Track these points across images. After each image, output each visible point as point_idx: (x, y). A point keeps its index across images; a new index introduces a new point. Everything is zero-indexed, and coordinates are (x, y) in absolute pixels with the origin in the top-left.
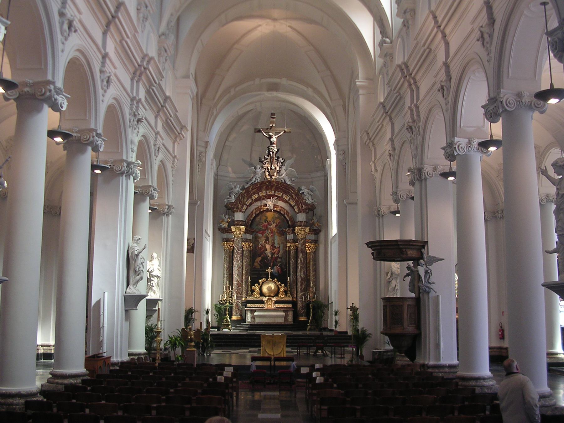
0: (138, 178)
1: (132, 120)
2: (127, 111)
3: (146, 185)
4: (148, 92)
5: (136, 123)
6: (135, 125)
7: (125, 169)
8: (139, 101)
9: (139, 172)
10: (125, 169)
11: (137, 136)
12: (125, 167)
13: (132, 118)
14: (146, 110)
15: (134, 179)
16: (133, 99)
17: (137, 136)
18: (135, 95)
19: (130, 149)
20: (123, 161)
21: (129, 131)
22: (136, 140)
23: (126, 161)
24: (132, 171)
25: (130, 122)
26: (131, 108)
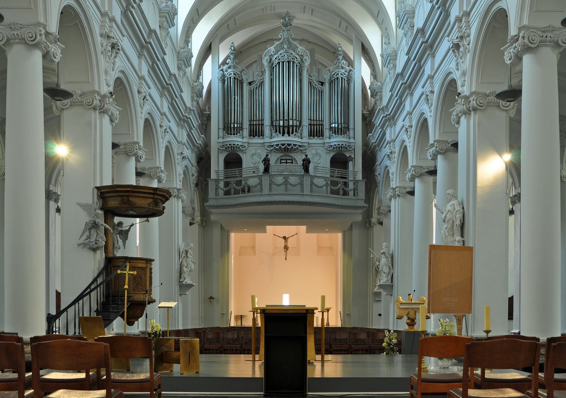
0: (116, 119)
1: (104, 45)
2: (97, 30)
3: (131, 141)
4: (125, 14)
5: (110, 48)
6: (109, 51)
7: (96, 102)
8: (112, 20)
9: (118, 113)
10: (96, 102)
11: (113, 70)
12: (98, 101)
13: (105, 42)
14: (123, 36)
15: (112, 121)
16: (104, 15)
17: (113, 70)
18: (106, 9)
19: (104, 81)
20: (95, 92)
21: (101, 58)
22: (114, 75)
23: (99, 93)
24: (107, 107)
25: (102, 46)
26: (102, 27)
